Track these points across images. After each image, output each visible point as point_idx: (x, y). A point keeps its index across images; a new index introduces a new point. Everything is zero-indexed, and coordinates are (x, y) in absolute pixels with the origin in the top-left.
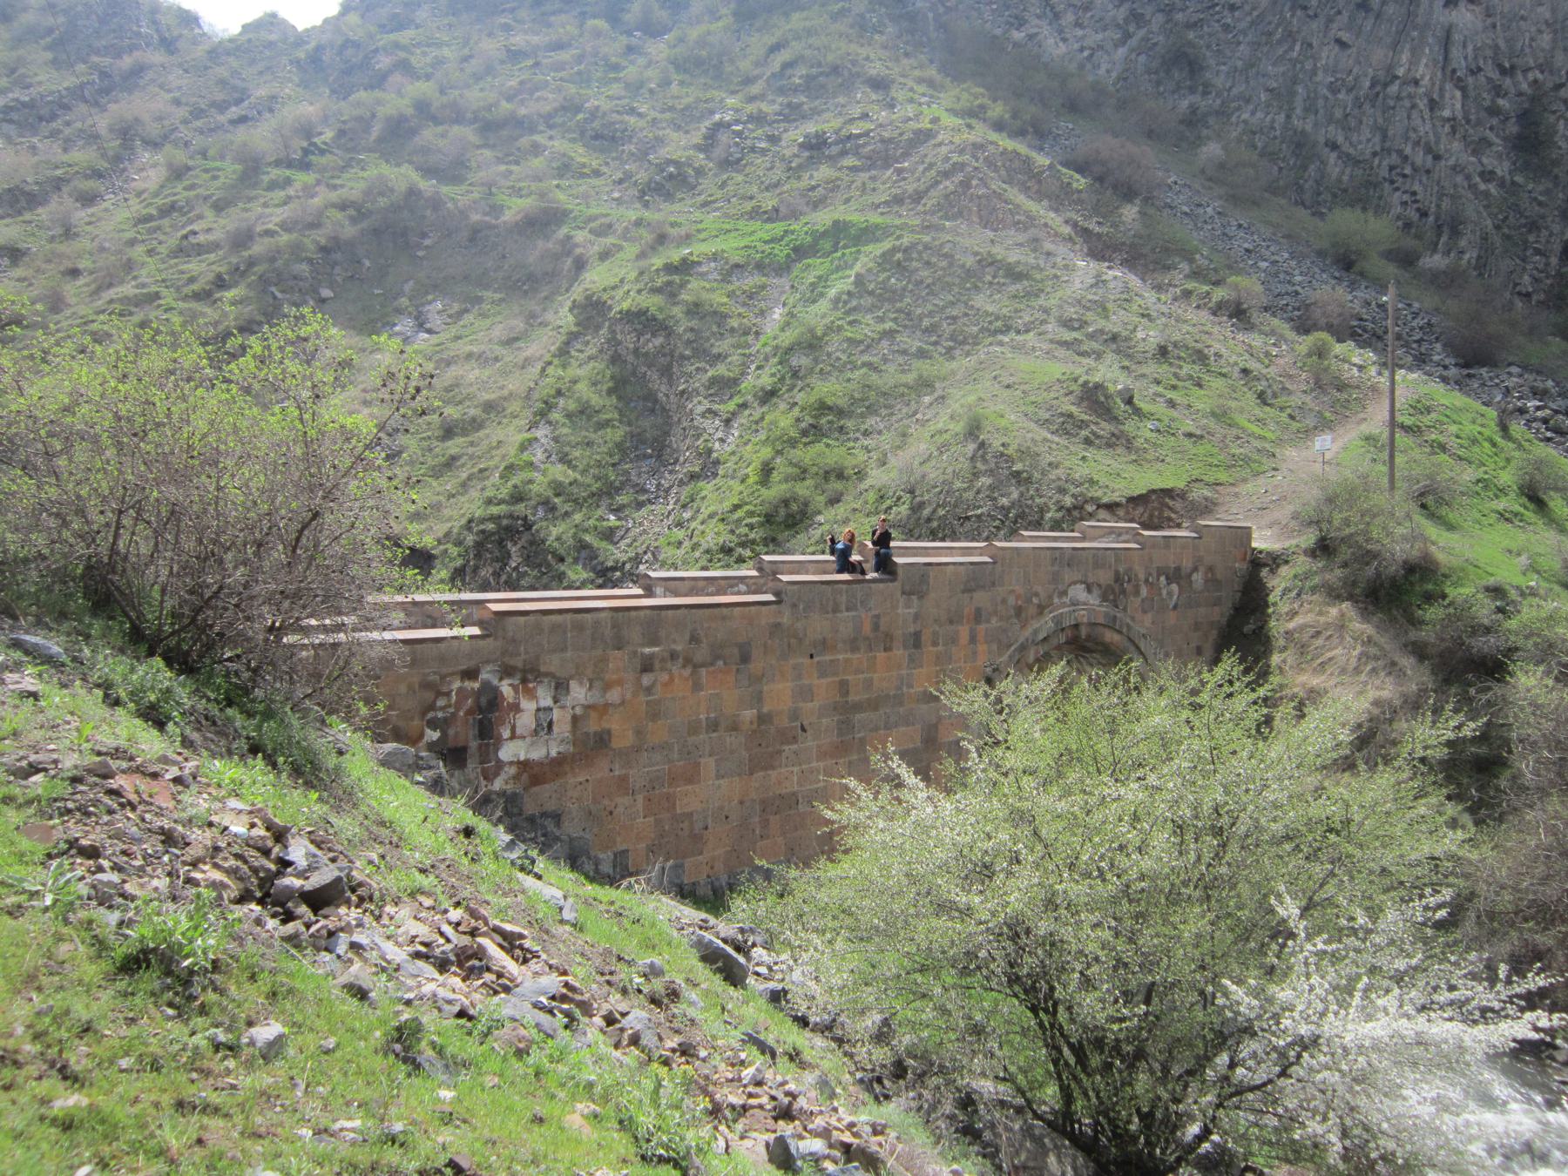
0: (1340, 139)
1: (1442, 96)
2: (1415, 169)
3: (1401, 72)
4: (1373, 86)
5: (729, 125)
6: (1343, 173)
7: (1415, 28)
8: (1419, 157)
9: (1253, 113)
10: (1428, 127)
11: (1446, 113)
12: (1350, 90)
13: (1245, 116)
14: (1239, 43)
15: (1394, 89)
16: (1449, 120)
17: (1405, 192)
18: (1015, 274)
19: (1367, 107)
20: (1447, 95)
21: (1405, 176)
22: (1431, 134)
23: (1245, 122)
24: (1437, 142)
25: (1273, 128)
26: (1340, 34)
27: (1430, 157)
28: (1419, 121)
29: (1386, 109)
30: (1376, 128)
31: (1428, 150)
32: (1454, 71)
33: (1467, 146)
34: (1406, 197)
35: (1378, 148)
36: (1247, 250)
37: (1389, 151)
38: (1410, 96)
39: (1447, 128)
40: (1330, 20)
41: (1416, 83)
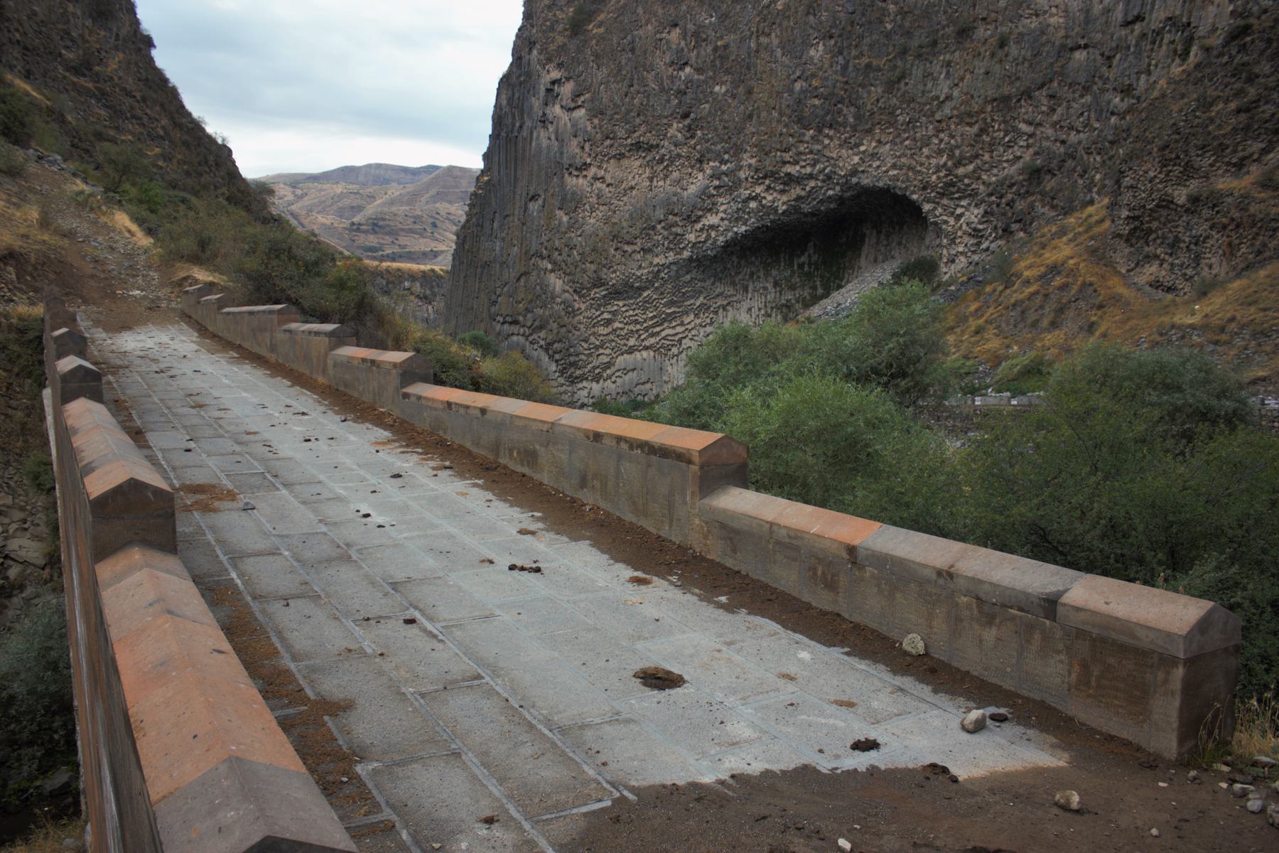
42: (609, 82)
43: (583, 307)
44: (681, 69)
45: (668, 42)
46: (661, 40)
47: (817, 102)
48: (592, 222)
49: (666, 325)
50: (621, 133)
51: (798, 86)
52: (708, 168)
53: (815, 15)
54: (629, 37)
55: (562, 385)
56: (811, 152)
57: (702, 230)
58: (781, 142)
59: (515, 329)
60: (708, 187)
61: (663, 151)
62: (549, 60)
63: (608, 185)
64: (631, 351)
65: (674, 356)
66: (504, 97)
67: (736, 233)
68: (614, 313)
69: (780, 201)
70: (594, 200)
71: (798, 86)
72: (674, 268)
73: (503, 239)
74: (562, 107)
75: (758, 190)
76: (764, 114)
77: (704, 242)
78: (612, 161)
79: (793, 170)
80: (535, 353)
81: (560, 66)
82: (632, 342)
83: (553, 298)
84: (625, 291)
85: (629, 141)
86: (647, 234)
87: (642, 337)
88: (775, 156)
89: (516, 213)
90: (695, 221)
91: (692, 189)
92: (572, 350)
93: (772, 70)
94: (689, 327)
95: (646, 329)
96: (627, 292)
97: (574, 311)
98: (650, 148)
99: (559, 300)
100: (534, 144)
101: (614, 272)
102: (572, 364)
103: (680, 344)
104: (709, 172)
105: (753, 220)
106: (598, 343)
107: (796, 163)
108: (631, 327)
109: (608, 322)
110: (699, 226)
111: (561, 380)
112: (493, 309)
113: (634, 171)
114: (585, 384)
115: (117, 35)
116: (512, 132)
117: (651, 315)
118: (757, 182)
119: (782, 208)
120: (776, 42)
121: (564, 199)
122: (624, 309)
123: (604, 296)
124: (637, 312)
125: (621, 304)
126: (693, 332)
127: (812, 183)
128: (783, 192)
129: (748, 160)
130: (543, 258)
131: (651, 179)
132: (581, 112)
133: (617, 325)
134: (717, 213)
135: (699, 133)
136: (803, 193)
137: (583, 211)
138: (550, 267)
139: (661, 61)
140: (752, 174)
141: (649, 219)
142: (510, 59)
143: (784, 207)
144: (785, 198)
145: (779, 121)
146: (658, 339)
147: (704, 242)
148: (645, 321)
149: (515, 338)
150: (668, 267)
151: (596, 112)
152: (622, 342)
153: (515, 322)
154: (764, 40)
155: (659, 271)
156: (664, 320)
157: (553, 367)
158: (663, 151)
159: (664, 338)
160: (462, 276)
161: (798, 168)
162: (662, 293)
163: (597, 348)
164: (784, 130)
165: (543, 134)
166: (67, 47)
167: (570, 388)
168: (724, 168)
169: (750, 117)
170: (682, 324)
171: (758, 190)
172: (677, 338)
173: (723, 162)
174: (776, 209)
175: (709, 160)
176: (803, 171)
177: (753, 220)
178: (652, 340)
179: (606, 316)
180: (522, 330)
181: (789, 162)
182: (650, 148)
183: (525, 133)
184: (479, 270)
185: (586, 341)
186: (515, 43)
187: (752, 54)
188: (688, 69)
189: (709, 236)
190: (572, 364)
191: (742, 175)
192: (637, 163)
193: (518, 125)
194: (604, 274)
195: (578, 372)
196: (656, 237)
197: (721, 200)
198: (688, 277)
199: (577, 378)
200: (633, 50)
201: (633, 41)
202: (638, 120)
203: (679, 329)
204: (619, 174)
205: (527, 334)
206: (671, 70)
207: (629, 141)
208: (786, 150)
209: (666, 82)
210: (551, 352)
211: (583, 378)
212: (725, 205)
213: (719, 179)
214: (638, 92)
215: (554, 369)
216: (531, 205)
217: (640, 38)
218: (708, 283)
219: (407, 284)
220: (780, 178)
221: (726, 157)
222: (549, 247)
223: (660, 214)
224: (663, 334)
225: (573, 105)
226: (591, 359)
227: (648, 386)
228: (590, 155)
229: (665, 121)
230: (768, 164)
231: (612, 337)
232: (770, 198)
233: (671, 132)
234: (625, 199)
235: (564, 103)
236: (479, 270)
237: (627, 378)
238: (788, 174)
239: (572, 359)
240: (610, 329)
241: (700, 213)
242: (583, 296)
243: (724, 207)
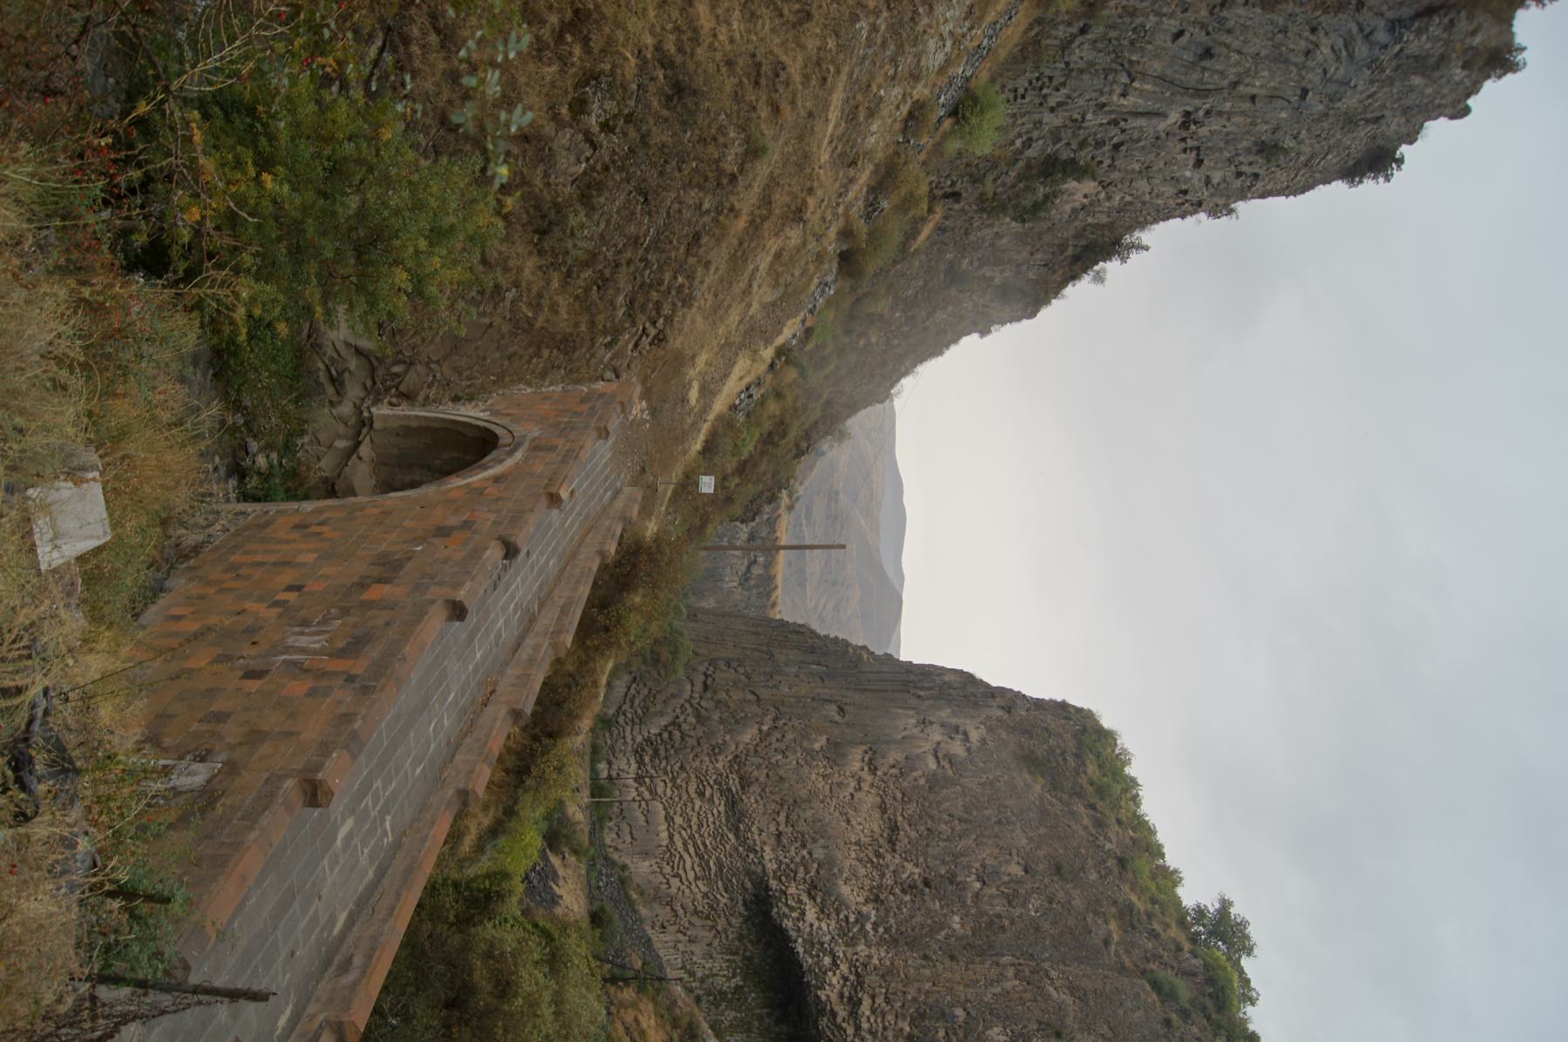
0: (1089, 36)
1: (1107, 112)
2: (1045, 96)
3: (1136, 84)
4: (1130, 62)
7: (1172, 94)
15: (1124, 79)
16: (1083, 118)
17: (1026, 90)
19: (1113, 56)
24: (1066, 111)
26: (1187, 35)
30: (1091, 64)
31: (1060, 104)
32: (1126, 120)
33: (1057, 128)
34: (1021, 91)
35: (1072, 66)
39: (1076, 116)
40: (1203, 26)
42: (965, 796)
43: (720, 765)
44: (979, 878)
45: (1007, 862)
46: (1010, 854)
47: (941, 1034)
48: (815, 778)
49: (697, 860)
50: (911, 809)
51: (959, 1012)
52: (869, 910)
53: (1038, 1030)
54: (1014, 818)
55: (633, 740)
56: (885, 1028)
57: (800, 901)
58: (895, 994)
59: (699, 687)
60: (848, 908)
61: (888, 857)
62: (990, 729)
63: (852, 795)
64: (669, 819)
65: (661, 868)
66: (953, 677)
67: (796, 941)
68: (711, 800)
69: (831, 990)
70: (836, 779)
71: (959, 1012)
72: (759, 870)
73: (797, 676)
74: (939, 743)
75: (844, 967)
76: (927, 972)
77: (787, 905)
78: (878, 799)
79: (865, 1008)
80: (670, 710)
81: (983, 741)
82: (678, 820)
83: (730, 732)
84: (736, 815)
85: (900, 819)
86: (796, 838)
87: (683, 832)
88: (880, 986)
89: (826, 691)
90: (809, 894)
91: (845, 890)
92: (672, 752)
93: (978, 981)
94: (693, 886)
95: (692, 837)
96: (734, 815)
97: (715, 754)
98: (892, 842)
99: (728, 737)
100: (900, 711)
101: (756, 802)
102: (656, 752)
103: (674, 876)
104: (865, 909)
105: (810, 961)
106: (678, 781)
107: (873, 1011)
108: (694, 820)
109: (701, 794)
110: (805, 898)
111: (639, 739)
112: (722, 664)
113: (867, 823)
114: (634, 765)
115: (987, 307)
116: (915, 687)
117: (707, 842)
118: (852, 965)
119: (822, 995)
120: (1008, 985)
121: (837, 745)
122: (715, 811)
123: (729, 790)
124: (712, 826)
125: (722, 808)
126: (687, 891)
127: (850, 1031)
128: (841, 995)
129: (879, 956)
130: (774, 721)
131: (858, 843)
132: (932, 765)
133: (698, 803)
134: (818, 919)
135: (908, 898)
136: (839, 1020)
137: (825, 767)
138: (765, 728)
139: (986, 854)
140: (861, 960)
141: (814, 840)
142: (994, 684)
143: (824, 998)
144: (834, 997)
145: (919, 990)
146: (681, 850)
147: (787, 905)
148: (701, 836)
149: (688, 687)
150: (760, 863)
151: (933, 782)
152: (678, 809)
153: (706, 687)
154: (1010, 972)
155: (756, 852)
156: (701, 858)
157: (654, 731)
158: (888, 857)
159: (681, 857)
160: (759, 629)
161: (868, 1013)
162: (731, 856)
163: (674, 779)
164: (910, 997)
165: (913, 721)
166: (971, 263)
167: (630, 748)
168: (869, 927)
169: (925, 957)
170: (697, 878)
171: (844, 967)
172: (681, 872)
173: (875, 926)
174: (822, 988)
175: (878, 910)
176: (864, 1020)
177: (810, 961)
178: (679, 844)
179: (708, 793)
180: (696, 695)
181: (874, 1002)
182: (892, 842)
183: (913, 701)
184: (765, 648)
185: (682, 767)
186: (1011, 690)
187: (995, 959)
188: (978, 885)
189: (792, 909)
190: (656, 752)
191: (861, 947)
192: (876, 828)
193: (922, 693)
194: (755, 788)
195: (647, 759)
196: (793, 849)
197: (833, 923)
198: (749, 885)
199: (641, 756)
200: (999, 822)
201: (1009, 823)
202: (923, 828)
203: (691, 875)
204: (865, 808)
205: (693, 701)
206: (977, 865)
207: (900, 819)
208: (887, 1000)
209: (964, 860)
210: (670, 728)
211: (640, 763)
212: (827, 927)
213: (857, 921)
214: (953, 829)
215: (652, 731)
216: (834, 707)
217: (1012, 831)
218: (741, 908)
219: (761, 559)
220: (856, 992)
221: (881, 930)
222: (786, 728)
223: (819, 854)
224: (686, 856)
225: (940, 755)
226: (661, 772)
227: (628, 839)
228: (885, 774)
229: (921, 859)
230: (872, 979)
231: (685, 797)
232: (834, 981)
233: (909, 866)
234: (837, 814)
235: (942, 745)
236: (765, 648)
237: (638, 814)
238: (860, 1002)
239: (662, 752)
240: (693, 795)
241: (819, 900)
242: (731, 766)
243: (825, 928)
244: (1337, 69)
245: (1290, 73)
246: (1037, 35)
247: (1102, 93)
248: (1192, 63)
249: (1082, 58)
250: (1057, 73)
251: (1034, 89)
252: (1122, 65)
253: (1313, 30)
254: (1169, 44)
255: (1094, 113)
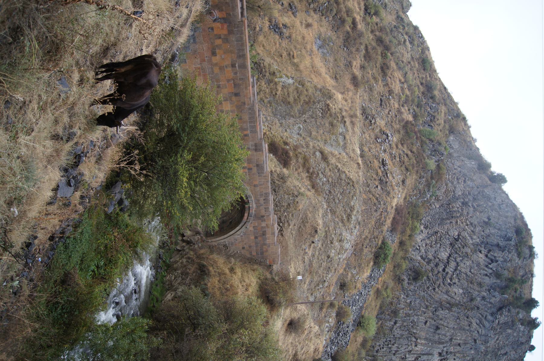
0: (398, 325)
3: (419, 341)
4: (414, 333)
5: (388, 138)
6: (387, 326)
7: (432, 344)
8: (394, 348)
9: (404, 298)
10: (403, 351)
11: (407, 356)
12: (412, 327)
13: (402, 296)
14: (424, 292)
16: (406, 357)
17: (383, 345)
18: (349, 217)
20: (412, 355)
21: (388, 345)
22: (400, 352)
23: (401, 296)
24: (399, 354)
25: (399, 305)
27: (394, 352)
28: (404, 348)
29: (407, 338)
31: (396, 351)
32: (420, 357)
34: (382, 346)
36: (362, 293)
37: (395, 340)
38: (411, 344)
40: (432, 319)
41: (416, 346)
244: (482, 331)
245: (467, 333)
246: (381, 324)
247: (409, 345)
248: (434, 332)
249: (398, 333)
250: (392, 339)
251: (386, 345)
252: (412, 335)
253: (467, 317)
254: (424, 326)
255: (409, 354)
